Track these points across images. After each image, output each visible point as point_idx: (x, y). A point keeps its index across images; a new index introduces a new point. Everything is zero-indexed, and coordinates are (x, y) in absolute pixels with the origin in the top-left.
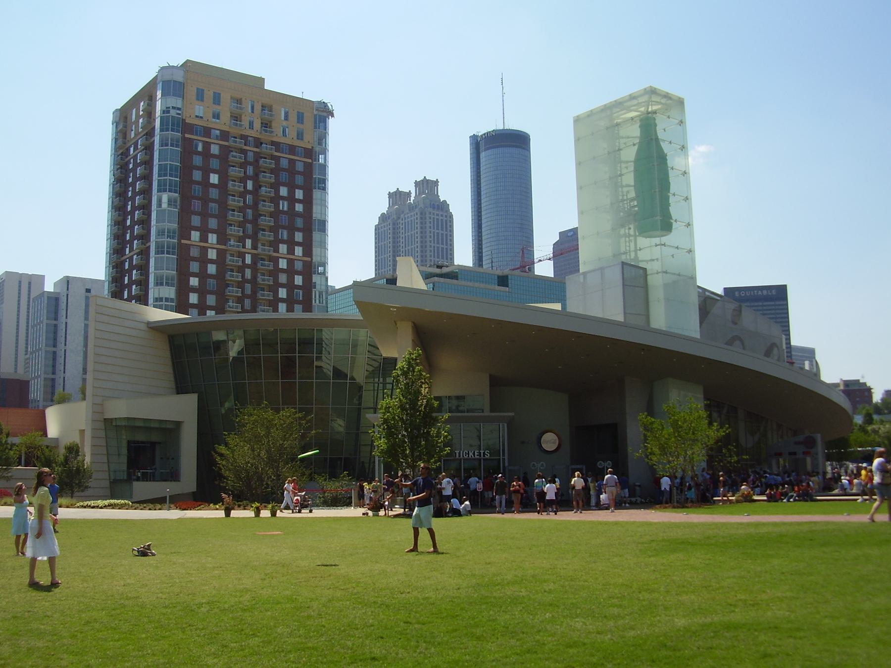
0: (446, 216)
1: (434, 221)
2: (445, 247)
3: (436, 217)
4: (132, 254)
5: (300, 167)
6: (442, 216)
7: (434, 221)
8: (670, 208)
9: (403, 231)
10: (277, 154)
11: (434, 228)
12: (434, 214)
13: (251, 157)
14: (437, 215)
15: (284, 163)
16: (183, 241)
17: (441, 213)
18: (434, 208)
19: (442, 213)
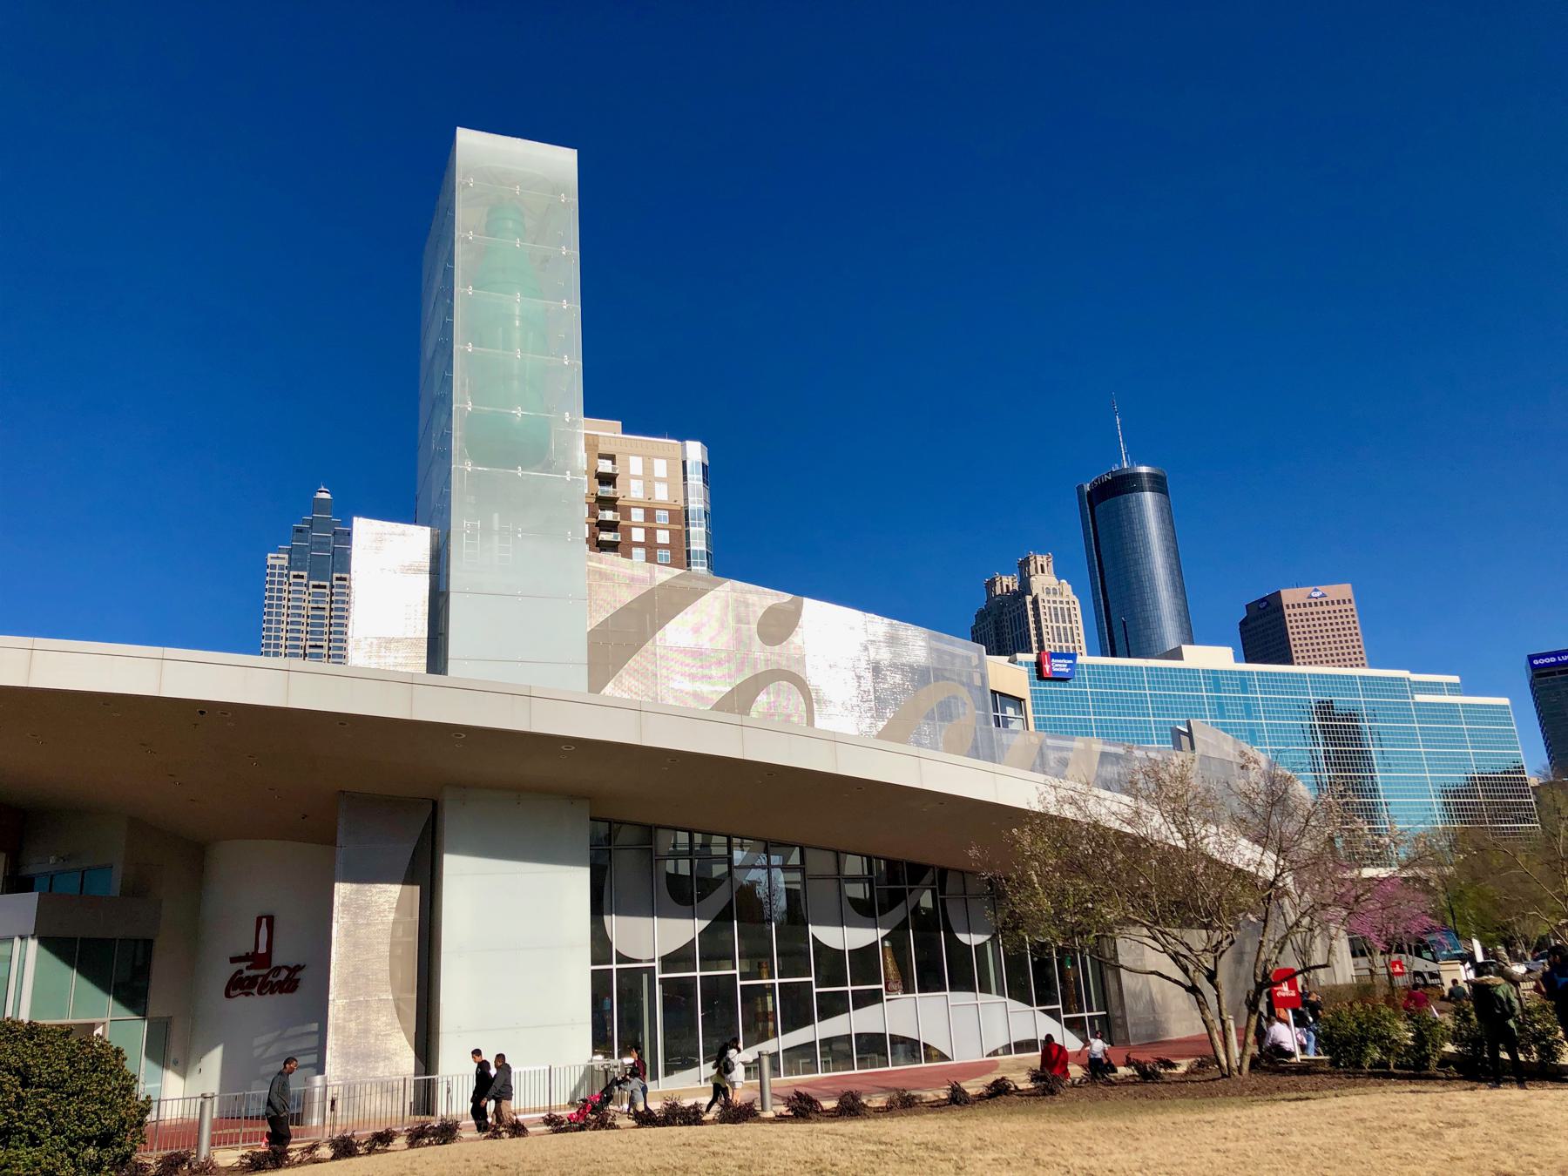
0: (1068, 603)
3: (1052, 605)
5: (663, 537)
6: (1061, 602)
9: (1010, 630)
10: (623, 523)
11: (1051, 621)
12: (1049, 602)
14: (1055, 602)
15: (638, 535)
17: (1058, 599)
18: (1048, 593)
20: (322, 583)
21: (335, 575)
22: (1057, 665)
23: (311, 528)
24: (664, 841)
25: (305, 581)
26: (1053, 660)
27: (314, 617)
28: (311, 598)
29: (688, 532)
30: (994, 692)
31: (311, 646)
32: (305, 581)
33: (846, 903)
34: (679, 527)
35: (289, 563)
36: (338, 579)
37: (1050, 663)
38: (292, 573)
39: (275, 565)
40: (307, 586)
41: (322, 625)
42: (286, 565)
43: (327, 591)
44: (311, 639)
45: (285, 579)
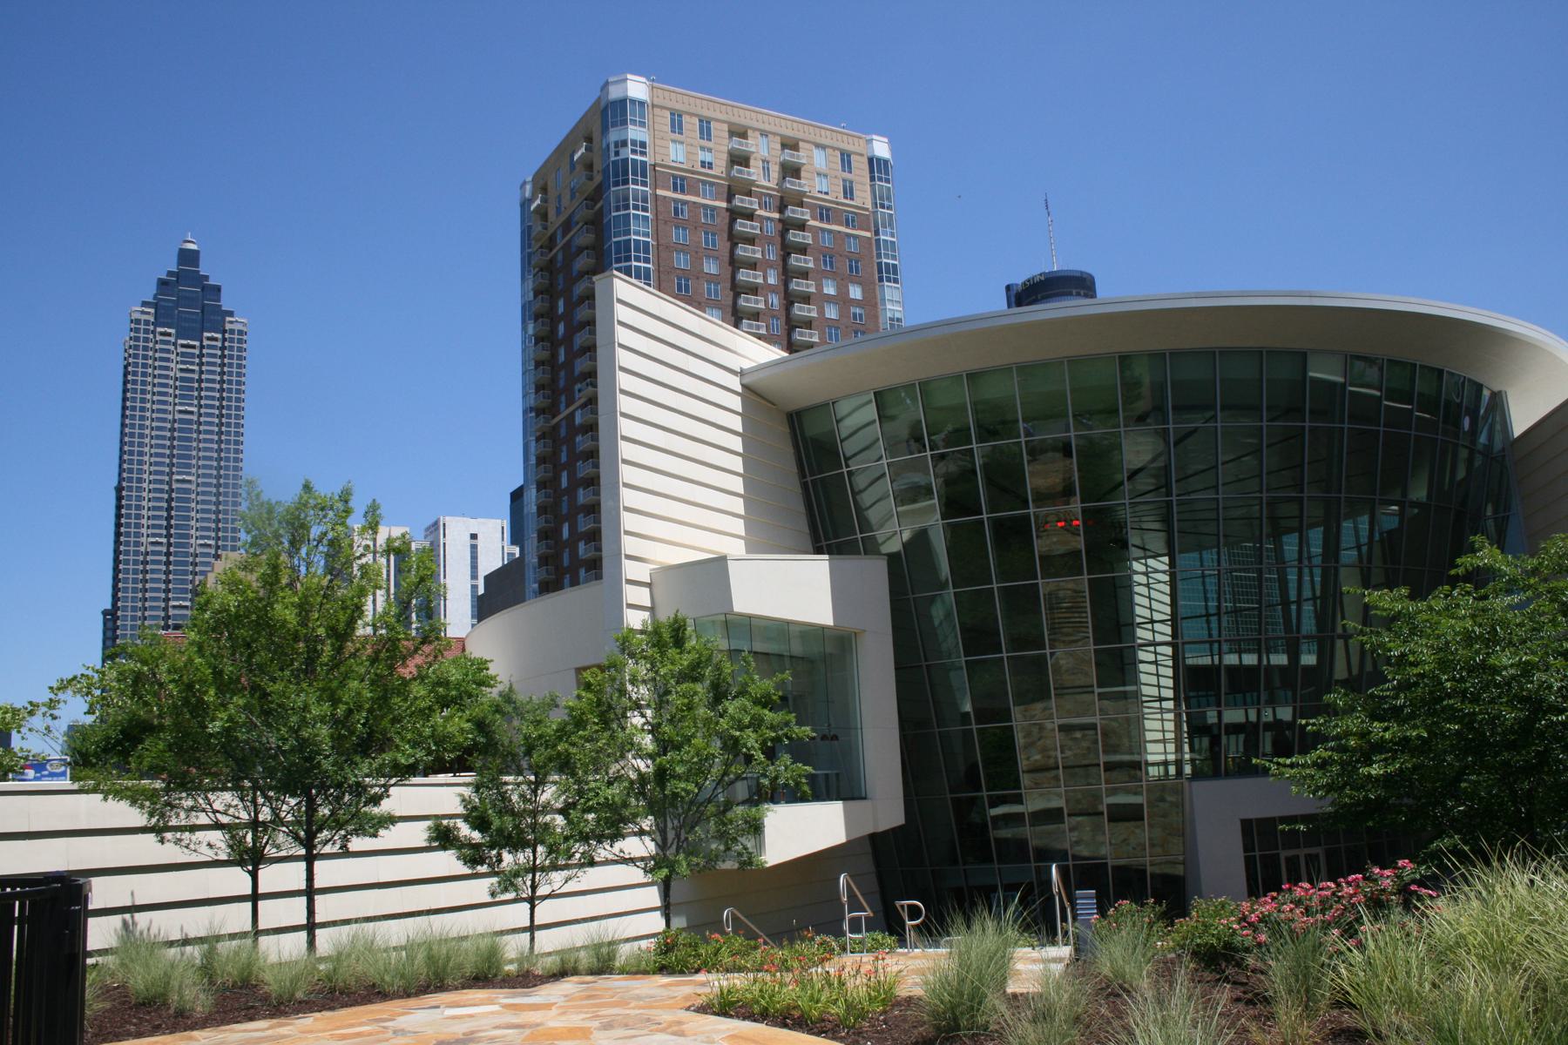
4: (571, 409)
13: (772, 229)
23: (177, 281)
25: (172, 339)
27: (183, 379)
28: (179, 359)
29: (878, 241)
32: (172, 339)
34: (868, 234)
35: (155, 319)
39: (140, 320)
40: (175, 344)
41: (191, 389)
42: (152, 320)
44: (181, 404)
45: (151, 336)
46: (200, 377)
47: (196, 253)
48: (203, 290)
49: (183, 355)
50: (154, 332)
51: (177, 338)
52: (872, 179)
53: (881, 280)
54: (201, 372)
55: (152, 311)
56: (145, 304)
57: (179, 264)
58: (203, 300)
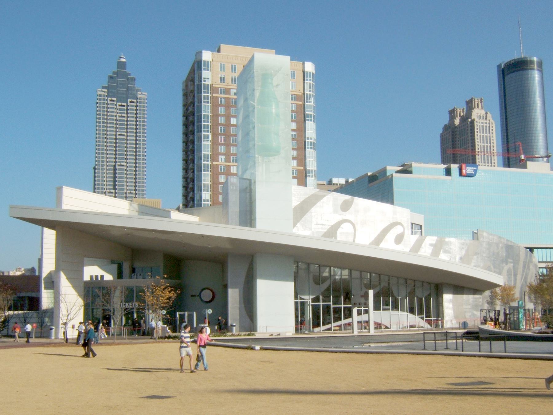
0: (489, 123)
1: (480, 127)
2: (489, 145)
6: (486, 123)
7: (480, 127)
8: (448, 120)
12: (479, 123)
14: (482, 123)
16: (214, 163)
17: (485, 121)
19: (482, 121)
20: (123, 104)
21: (129, 100)
22: (469, 170)
24: (312, 267)
25: (115, 103)
26: (467, 168)
28: (118, 111)
29: (304, 105)
30: (412, 224)
31: (119, 135)
32: (115, 103)
33: (362, 285)
34: (301, 103)
35: (108, 94)
36: (131, 102)
37: (466, 169)
38: (110, 99)
39: (101, 95)
40: (116, 105)
42: (106, 94)
43: (125, 108)
46: (127, 119)
47: (124, 63)
48: (128, 80)
49: (120, 110)
50: (107, 100)
51: (117, 102)
52: (304, 80)
53: (305, 120)
54: (128, 117)
55: (106, 90)
56: (104, 87)
57: (118, 68)
58: (128, 84)
